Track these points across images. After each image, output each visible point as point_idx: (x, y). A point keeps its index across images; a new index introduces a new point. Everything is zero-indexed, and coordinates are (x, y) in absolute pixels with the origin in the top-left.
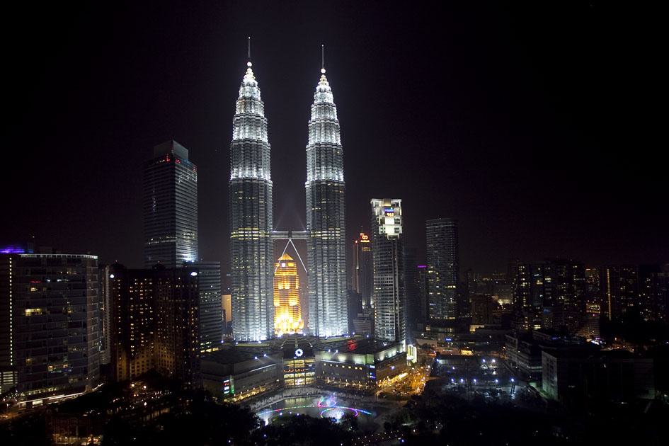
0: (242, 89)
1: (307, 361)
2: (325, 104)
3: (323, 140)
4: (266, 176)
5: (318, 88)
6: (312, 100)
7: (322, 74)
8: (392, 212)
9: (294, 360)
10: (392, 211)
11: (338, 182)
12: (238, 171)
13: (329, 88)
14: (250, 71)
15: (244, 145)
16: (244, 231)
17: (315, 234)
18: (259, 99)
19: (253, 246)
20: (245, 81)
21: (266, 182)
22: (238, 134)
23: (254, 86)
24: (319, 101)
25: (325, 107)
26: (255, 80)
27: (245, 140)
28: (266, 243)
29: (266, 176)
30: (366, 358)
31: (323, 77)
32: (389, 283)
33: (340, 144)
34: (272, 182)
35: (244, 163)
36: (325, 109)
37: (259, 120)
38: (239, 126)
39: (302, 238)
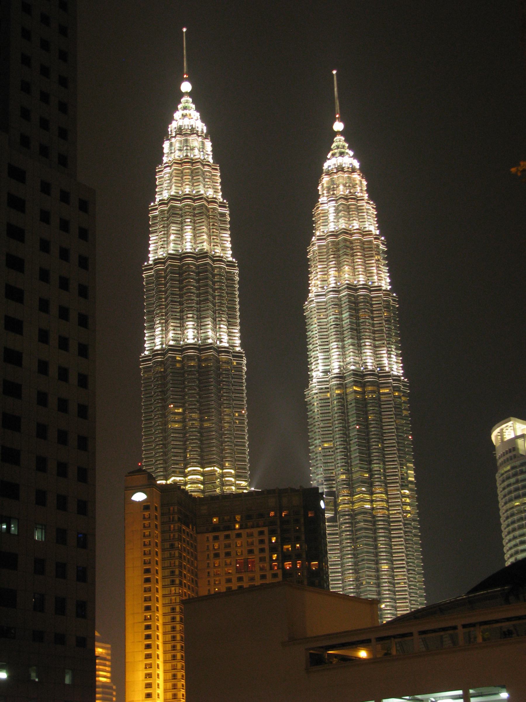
2: (193, 162)
5: (173, 126)
7: (182, 95)
36: (193, 173)
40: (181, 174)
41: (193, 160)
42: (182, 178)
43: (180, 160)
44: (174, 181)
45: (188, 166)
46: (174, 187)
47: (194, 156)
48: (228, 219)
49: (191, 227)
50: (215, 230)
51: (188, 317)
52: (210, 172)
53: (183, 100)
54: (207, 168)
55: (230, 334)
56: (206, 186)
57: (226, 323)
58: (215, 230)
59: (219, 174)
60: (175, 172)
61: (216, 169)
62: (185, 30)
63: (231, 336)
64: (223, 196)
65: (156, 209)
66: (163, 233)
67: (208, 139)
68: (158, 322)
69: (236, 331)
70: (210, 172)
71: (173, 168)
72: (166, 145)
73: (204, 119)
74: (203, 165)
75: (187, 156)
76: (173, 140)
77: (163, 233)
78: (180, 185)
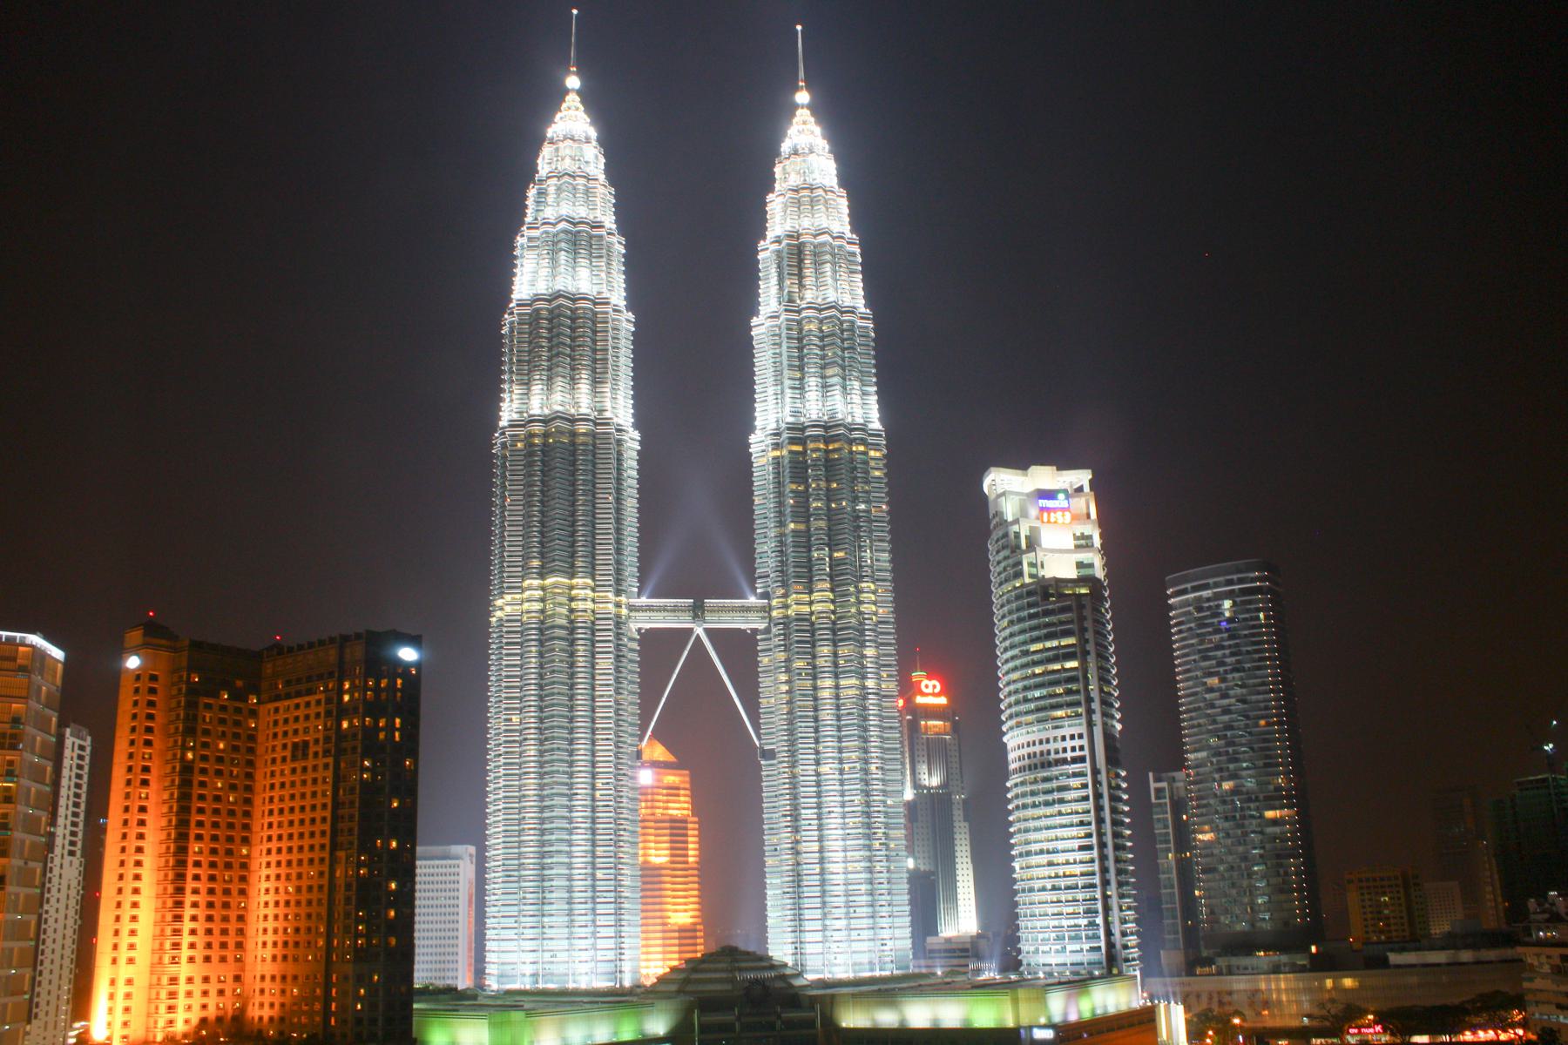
0: (547, 151)
2: (811, 189)
4: (620, 408)
5: (786, 147)
8: (1063, 510)
10: (1065, 504)
12: (527, 394)
14: (573, 100)
15: (551, 311)
18: (602, 177)
19: (572, 642)
23: (588, 141)
24: (794, 180)
25: (806, 196)
29: (621, 412)
30: (1015, 1001)
32: (1069, 755)
33: (863, 310)
34: (636, 435)
40: (798, 203)
42: (799, 208)
44: (788, 212)
45: (806, 193)
46: (788, 220)
48: (859, 259)
52: (834, 200)
53: (799, 112)
54: (830, 195)
62: (799, 28)
65: (767, 249)
70: (834, 200)
71: (788, 196)
72: (778, 170)
74: (825, 191)
76: (787, 162)
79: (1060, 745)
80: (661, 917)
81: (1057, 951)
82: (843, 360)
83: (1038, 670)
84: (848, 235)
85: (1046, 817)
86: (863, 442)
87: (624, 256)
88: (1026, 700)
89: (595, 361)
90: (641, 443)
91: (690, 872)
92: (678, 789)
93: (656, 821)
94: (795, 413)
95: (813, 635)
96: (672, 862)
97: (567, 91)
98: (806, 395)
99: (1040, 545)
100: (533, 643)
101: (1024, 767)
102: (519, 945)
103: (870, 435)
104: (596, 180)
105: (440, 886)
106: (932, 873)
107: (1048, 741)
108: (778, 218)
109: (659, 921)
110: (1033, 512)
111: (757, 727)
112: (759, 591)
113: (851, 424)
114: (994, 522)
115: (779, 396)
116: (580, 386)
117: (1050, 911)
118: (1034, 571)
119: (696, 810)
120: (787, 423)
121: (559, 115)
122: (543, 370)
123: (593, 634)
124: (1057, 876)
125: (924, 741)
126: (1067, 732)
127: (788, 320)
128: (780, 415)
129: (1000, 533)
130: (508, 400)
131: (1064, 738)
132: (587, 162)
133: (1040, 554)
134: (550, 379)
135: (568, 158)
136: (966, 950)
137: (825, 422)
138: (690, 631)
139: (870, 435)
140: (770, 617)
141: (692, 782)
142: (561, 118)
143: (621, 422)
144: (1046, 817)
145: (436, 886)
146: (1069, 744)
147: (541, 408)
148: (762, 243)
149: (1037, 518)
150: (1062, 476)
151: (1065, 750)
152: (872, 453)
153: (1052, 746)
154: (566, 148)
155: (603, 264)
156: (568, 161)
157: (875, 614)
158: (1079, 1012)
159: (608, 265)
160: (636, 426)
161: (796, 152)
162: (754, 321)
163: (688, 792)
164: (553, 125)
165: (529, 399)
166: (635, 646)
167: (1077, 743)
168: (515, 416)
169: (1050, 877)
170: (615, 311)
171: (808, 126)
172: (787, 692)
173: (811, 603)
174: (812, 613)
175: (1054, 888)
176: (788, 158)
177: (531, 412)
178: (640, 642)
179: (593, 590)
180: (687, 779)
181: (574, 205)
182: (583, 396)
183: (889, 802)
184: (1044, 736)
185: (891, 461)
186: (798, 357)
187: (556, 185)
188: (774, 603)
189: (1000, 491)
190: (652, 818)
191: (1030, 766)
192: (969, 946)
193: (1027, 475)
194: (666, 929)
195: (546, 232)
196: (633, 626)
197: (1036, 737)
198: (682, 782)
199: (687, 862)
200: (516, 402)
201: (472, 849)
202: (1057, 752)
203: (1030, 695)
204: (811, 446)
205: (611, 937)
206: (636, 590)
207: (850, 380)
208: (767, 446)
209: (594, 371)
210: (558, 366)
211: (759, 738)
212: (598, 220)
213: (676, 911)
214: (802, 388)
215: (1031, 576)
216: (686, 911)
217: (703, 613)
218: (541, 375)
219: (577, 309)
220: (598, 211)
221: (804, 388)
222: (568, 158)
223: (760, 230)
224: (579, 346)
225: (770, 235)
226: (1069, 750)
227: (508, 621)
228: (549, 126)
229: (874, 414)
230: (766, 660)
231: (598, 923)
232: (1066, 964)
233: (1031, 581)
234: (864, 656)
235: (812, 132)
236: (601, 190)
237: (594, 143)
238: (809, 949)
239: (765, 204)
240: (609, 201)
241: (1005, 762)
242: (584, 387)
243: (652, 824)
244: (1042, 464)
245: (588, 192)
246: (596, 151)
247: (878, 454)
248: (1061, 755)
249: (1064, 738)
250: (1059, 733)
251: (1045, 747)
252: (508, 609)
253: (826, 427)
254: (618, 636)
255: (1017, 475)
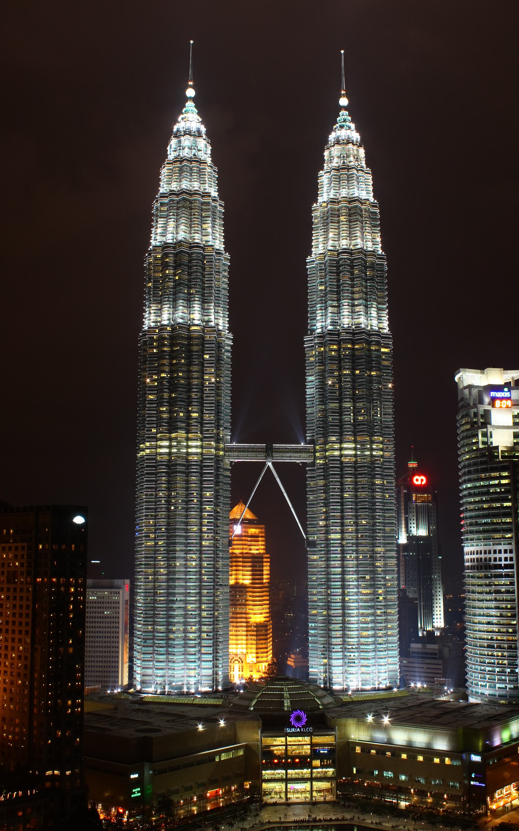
0: (173, 142)
1: (317, 740)
3: (344, 243)
5: (332, 137)
6: (319, 163)
7: (340, 108)
9: (286, 735)
10: (507, 395)
11: (378, 334)
13: (356, 136)
14: (190, 105)
16: (170, 439)
17: (326, 451)
18: (209, 160)
19: (188, 474)
20: (180, 126)
21: (219, 333)
22: (163, 235)
23: (200, 136)
24: (336, 163)
26: (202, 122)
27: (179, 243)
28: (217, 469)
31: (344, 114)
32: (503, 563)
33: (380, 252)
34: (231, 336)
35: (175, 294)
36: (349, 178)
37: (208, 204)
38: (167, 217)
39: (298, 459)
40: (339, 179)
41: (348, 166)
43: (338, 167)
44: (332, 185)
46: (332, 191)
47: (350, 162)
49: (346, 226)
50: (367, 228)
51: (343, 305)
55: (379, 318)
56: (360, 189)
57: (375, 309)
58: (367, 228)
59: (371, 178)
60: (333, 177)
61: (369, 173)
63: (380, 320)
64: (374, 197)
66: (323, 230)
67: (362, 147)
68: (319, 308)
69: (385, 315)
71: (332, 173)
72: (326, 153)
73: (358, 130)
74: (358, 170)
75: (344, 163)
76: (332, 149)
77: (323, 230)
78: (337, 188)
79: (498, 556)
80: (246, 618)
81: (490, 687)
82: (366, 288)
83: (485, 506)
84: (372, 200)
85: (487, 600)
86: (378, 343)
87: (224, 214)
88: (477, 524)
89: (203, 289)
90: (233, 340)
91: (264, 589)
92: (258, 537)
93: (244, 558)
94: (333, 323)
95: (342, 470)
96: (252, 583)
97: (186, 99)
98: (342, 317)
99: (490, 424)
100: (164, 474)
101: (474, 566)
102: (153, 664)
103: (383, 338)
104: (206, 163)
105: (107, 630)
106: (416, 599)
107: (490, 552)
108: (325, 189)
109: (244, 620)
110: (487, 400)
111: (305, 527)
112: (308, 438)
113: (369, 331)
114: (461, 404)
115: (324, 317)
116: (194, 305)
117: (487, 661)
118: (485, 439)
119: (268, 549)
120: (328, 330)
121: (181, 116)
122: (170, 294)
123: (202, 469)
124: (492, 639)
125: (414, 506)
126: (502, 547)
127: (330, 260)
128: (324, 324)
129: (465, 412)
130: (147, 313)
131: (500, 552)
132: (199, 150)
133: (490, 429)
134: (175, 301)
135: (187, 148)
136: (435, 654)
137: (353, 330)
138: (265, 462)
139: (383, 338)
140: (315, 455)
141: (266, 532)
142: (183, 119)
143: (221, 328)
144: (487, 600)
145: (105, 605)
146: (503, 555)
147: (169, 320)
148: (315, 205)
149: (489, 404)
150: (507, 373)
151: (500, 560)
152: (383, 350)
153: (492, 556)
154: (186, 141)
155: (210, 222)
156: (187, 150)
157: (382, 456)
158: (501, 739)
159: (214, 221)
160: (230, 329)
161: (338, 142)
162: (309, 259)
163: (263, 539)
164: (177, 124)
165: (161, 313)
166: (228, 474)
167: (508, 555)
168: (153, 325)
169: (488, 639)
170: (217, 253)
171: (348, 123)
172: (324, 513)
173: (341, 449)
174: (341, 456)
175: (489, 646)
176: (333, 146)
177: (162, 323)
178: (231, 471)
179: (202, 440)
180: (263, 530)
181: (191, 181)
182: (196, 312)
183: (387, 578)
184: (487, 548)
185: (395, 355)
186: (337, 285)
187: (178, 167)
188: (317, 447)
189: (465, 384)
190: (241, 555)
191: (477, 566)
192: (437, 651)
193: (483, 373)
194: (248, 626)
195: (173, 200)
196: (227, 461)
197: (482, 548)
198: (261, 532)
199: (262, 583)
200: (153, 315)
201: (127, 582)
202: (495, 559)
203: (479, 521)
204: (344, 346)
205: (211, 661)
206: (229, 437)
207: (370, 301)
208: (315, 344)
209: (203, 295)
210: (180, 292)
211: (306, 534)
212: (207, 191)
213: (255, 614)
214: (338, 307)
215: (484, 443)
216: (261, 614)
217: (272, 453)
218: (169, 298)
219: (193, 253)
220: (207, 185)
221: (340, 313)
222: (187, 148)
223: (314, 196)
224: (194, 279)
225: (320, 199)
226: (503, 559)
227: (147, 459)
228: (175, 124)
229: (385, 324)
230: (311, 497)
231: (203, 651)
232: (495, 695)
233: (483, 446)
234: (374, 484)
235: (349, 128)
236: (209, 170)
237: (204, 137)
238: (335, 670)
239: (317, 178)
240: (214, 177)
241: (463, 561)
242: (197, 307)
243: (241, 559)
244: (494, 367)
245: (200, 172)
246: (204, 142)
247: (386, 350)
248: (498, 563)
249: (500, 552)
250: (498, 548)
251: (488, 556)
252: (148, 451)
253: (353, 334)
254: (217, 469)
255: (477, 373)
